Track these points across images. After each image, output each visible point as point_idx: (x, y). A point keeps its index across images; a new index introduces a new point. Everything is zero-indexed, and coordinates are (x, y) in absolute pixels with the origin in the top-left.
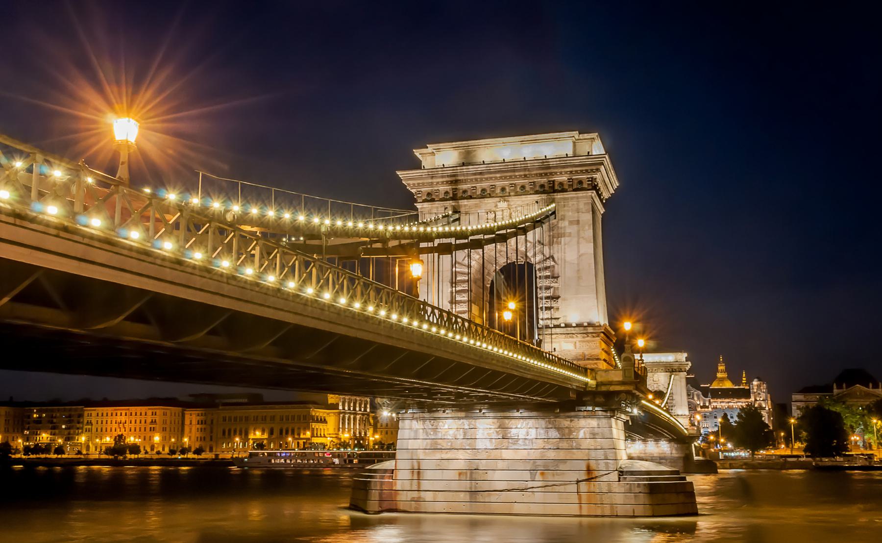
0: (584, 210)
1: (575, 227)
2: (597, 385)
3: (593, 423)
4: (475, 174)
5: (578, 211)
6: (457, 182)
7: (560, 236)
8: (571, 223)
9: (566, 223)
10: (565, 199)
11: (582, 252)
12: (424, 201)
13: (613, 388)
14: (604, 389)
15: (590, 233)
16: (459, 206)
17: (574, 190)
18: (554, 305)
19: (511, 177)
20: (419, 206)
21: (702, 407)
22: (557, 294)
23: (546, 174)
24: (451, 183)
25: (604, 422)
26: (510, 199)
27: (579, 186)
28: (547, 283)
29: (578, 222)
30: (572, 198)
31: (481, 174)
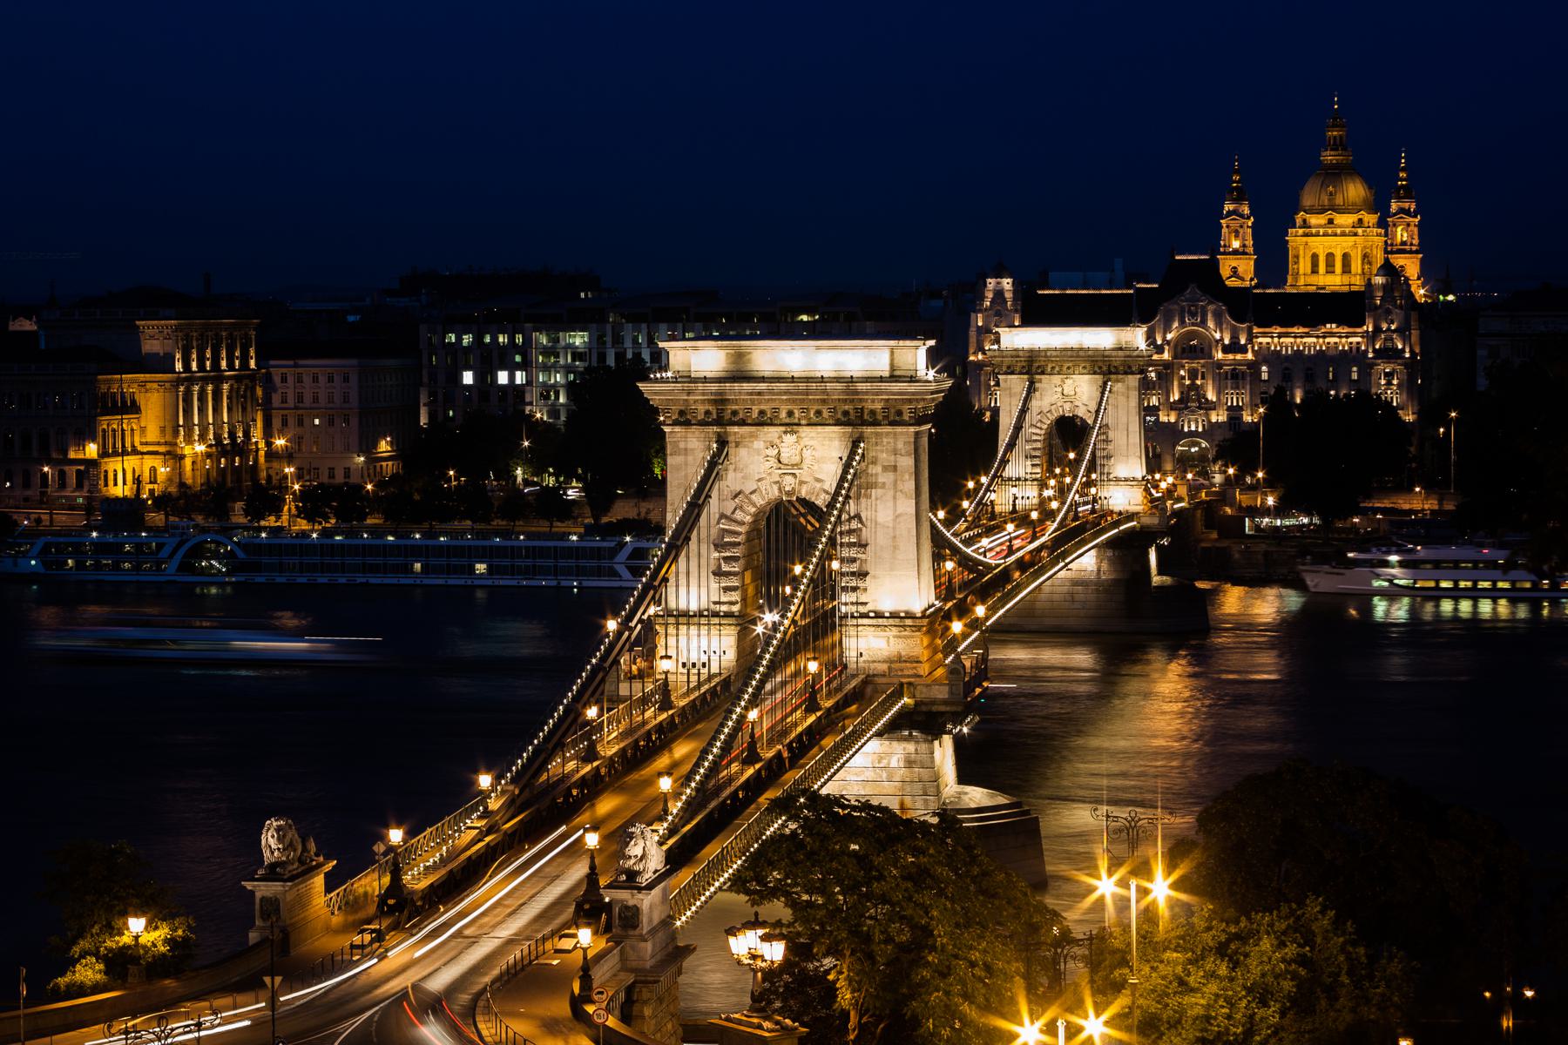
1: (890, 476)
2: (917, 704)
3: (911, 747)
5: (895, 452)
7: (870, 486)
8: (885, 469)
9: (878, 469)
10: (877, 434)
13: (935, 708)
14: (924, 708)
15: (911, 485)
17: (892, 423)
18: (861, 584)
20: (667, 429)
21: (1226, 350)
22: (865, 568)
24: (715, 402)
25: (923, 747)
26: (801, 429)
28: (853, 553)
29: (895, 468)
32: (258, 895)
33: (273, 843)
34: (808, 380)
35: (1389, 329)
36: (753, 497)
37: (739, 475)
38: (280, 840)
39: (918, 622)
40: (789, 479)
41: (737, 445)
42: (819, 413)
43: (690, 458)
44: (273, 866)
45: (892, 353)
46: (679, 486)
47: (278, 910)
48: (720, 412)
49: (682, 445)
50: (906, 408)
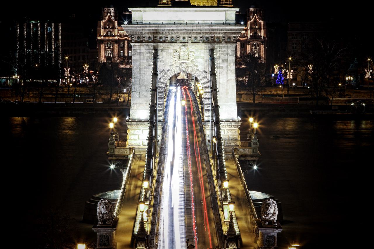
0: (231, 54)
4: (169, 30)
5: (227, 54)
6: (157, 33)
8: (223, 61)
10: (220, 47)
11: (229, 78)
12: (136, 42)
16: (157, 46)
17: (227, 42)
19: (190, 33)
23: (211, 33)
24: (154, 33)
26: (188, 44)
27: (229, 40)
29: (227, 61)
30: (224, 47)
31: (172, 30)
32: (99, 234)
33: (103, 211)
34: (192, 24)
35: (255, 28)
36: (168, 72)
37: (163, 63)
38: (107, 208)
39: (237, 124)
40: (184, 65)
41: (162, 51)
42: (196, 38)
43: (142, 56)
44: (104, 221)
45: (226, 13)
46: (137, 68)
47: (108, 241)
48: (155, 38)
49: (138, 51)
50: (232, 36)
